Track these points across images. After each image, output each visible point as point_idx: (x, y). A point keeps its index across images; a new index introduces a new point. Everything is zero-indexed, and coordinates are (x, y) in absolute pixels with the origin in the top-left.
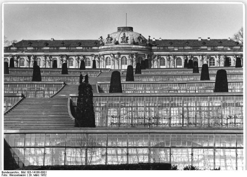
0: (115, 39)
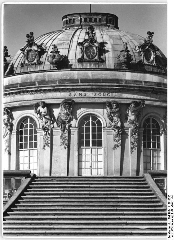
0: (55, 47)
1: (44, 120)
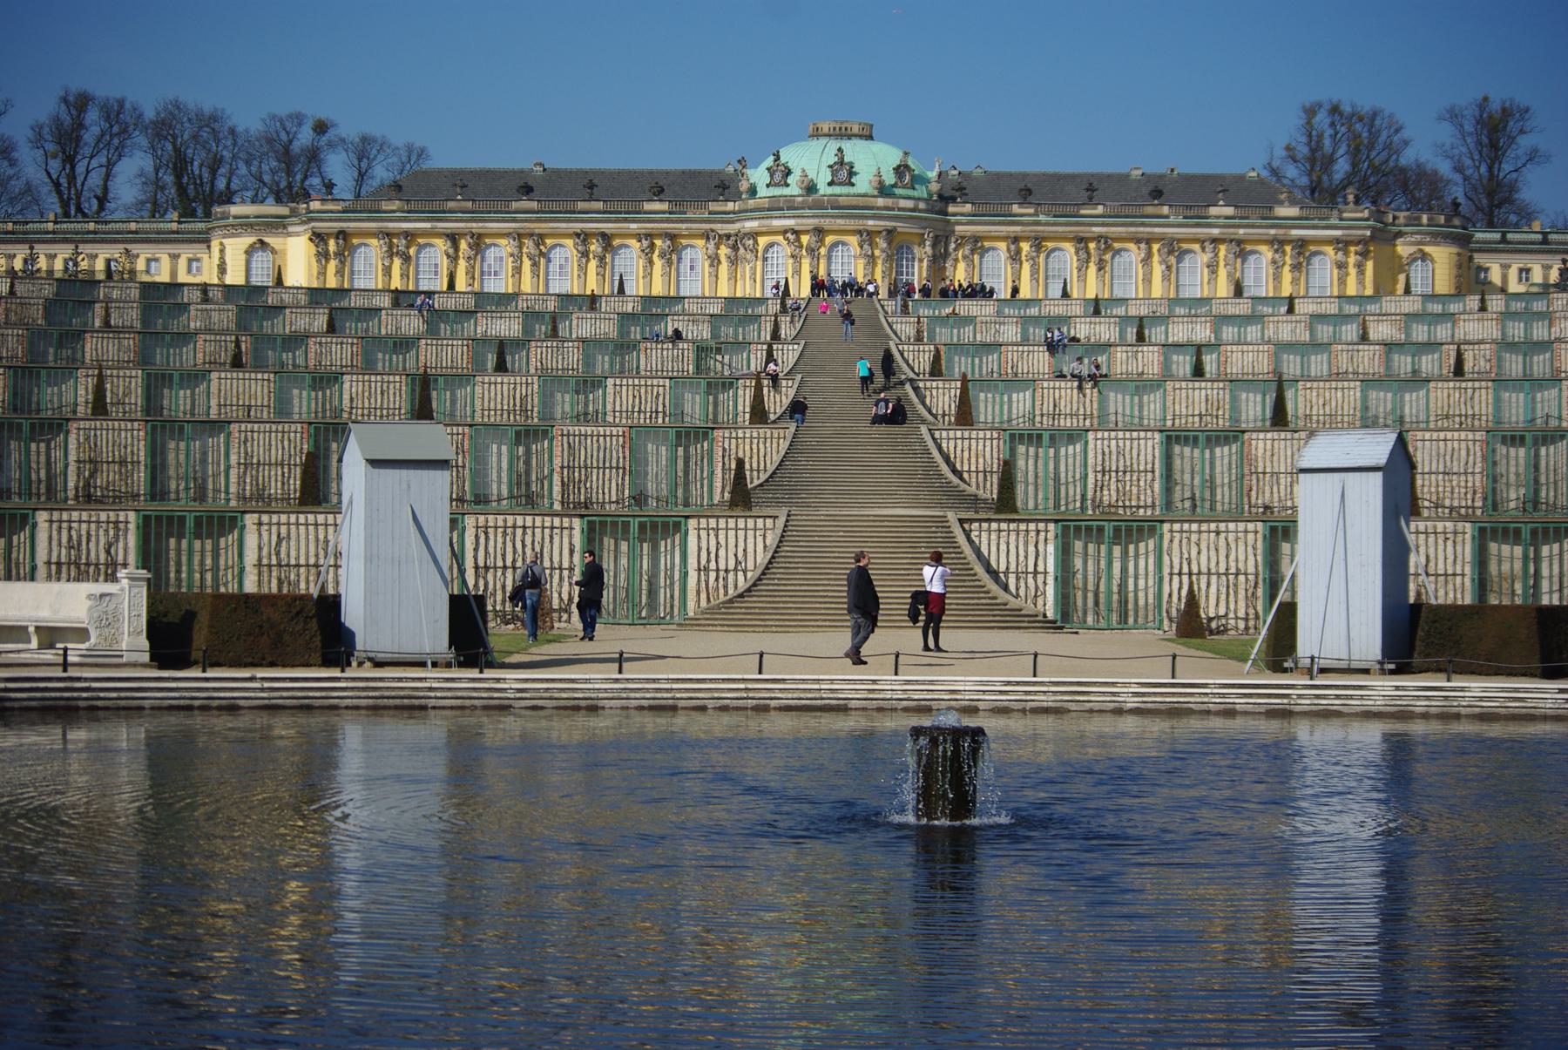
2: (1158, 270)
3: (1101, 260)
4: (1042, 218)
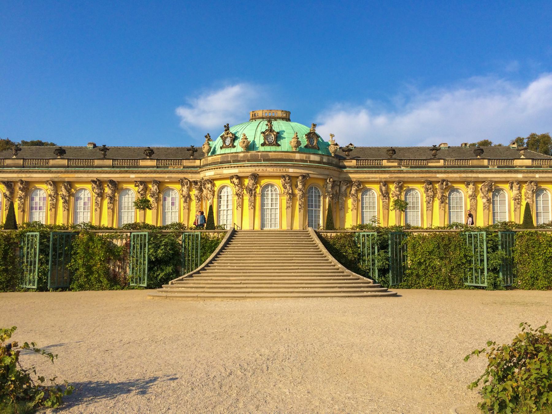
1: (237, 188)
2: (481, 201)
3: (443, 196)
4: (403, 168)
